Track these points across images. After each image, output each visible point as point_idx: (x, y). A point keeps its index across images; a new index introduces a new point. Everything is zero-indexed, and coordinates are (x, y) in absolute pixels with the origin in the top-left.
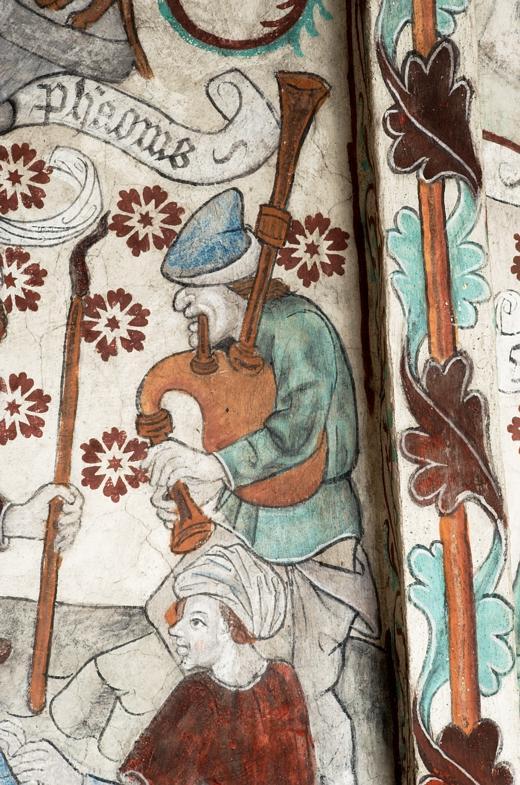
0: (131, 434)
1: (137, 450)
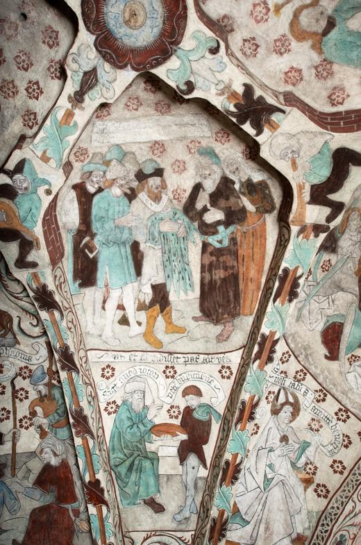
0: (29, 416)
1: (30, 419)
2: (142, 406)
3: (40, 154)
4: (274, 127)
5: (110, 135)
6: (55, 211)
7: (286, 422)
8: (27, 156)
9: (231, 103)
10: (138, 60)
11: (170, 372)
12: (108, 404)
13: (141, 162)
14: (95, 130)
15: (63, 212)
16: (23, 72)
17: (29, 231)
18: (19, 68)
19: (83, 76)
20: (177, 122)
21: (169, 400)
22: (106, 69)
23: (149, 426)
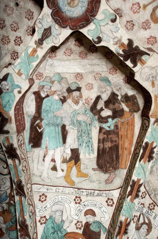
2: (60, 220)
3: (17, 71)
4: (143, 63)
5: (55, 68)
6: (23, 105)
7: (144, 235)
8: (10, 72)
9: (120, 49)
10: (73, 24)
11: (78, 200)
12: (41, 218)
13: (70, 83)
14: (48, 64)
15: (27, 106)
16: (14, 32)
17: (7, 113)
18: (12, 30)
19: (44, 31)
20: (90, 63)
21: (76, 218)
22: (56, 28)
23: (64, 233)
